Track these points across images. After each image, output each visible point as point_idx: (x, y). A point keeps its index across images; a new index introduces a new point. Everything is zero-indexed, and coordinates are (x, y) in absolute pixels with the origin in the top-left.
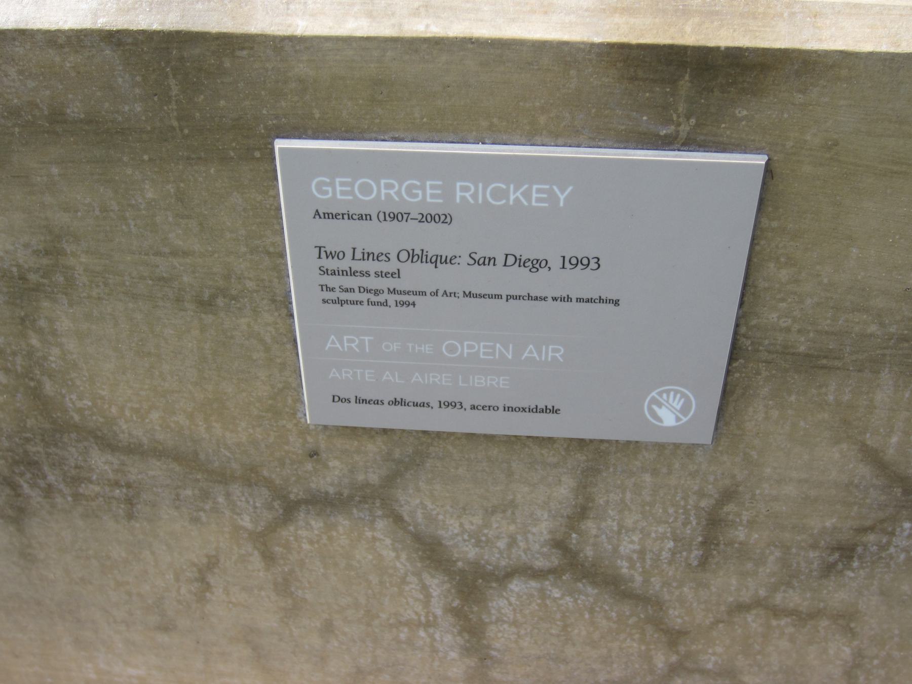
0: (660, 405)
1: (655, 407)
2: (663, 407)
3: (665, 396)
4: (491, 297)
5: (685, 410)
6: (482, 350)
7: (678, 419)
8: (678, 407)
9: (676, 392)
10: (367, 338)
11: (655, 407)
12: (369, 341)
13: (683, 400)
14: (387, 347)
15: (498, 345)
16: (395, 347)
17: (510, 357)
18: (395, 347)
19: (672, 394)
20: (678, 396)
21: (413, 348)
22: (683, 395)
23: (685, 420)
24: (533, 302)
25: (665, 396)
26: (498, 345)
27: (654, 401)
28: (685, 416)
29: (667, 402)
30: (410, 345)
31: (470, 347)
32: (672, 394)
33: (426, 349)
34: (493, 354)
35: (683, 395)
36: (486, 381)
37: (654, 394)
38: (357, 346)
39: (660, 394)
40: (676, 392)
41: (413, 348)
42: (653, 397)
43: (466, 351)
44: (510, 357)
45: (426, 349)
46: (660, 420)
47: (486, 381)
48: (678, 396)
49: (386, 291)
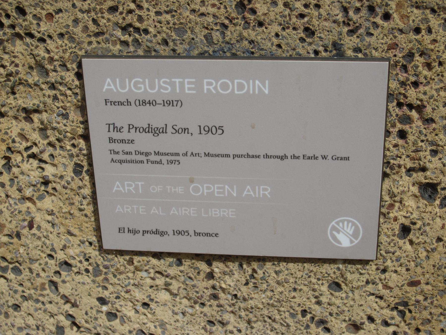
0: (338, 231)
1: (335, 233)
2: (341, 233)
3: (341, 224)
4: (223, 156)
5: (355, 234)
6: (216, 190)
7: (352, 242)
8: (351, 233)
9: (349, 221)
10: (140, 183)
11: (335, 233)
12: (141, 185)
13: (353, 228)
14: (154, 189)
15: (226, 187)
16: (158, 189)
17: (235, 195)
18: (158, 189)
19: (346, 223)
20: (350, 224)
21: (171, 189)
22: (354, 224)
23: (356, 242)
24: (251, 159)
25: (341, 224)
26: (226, 187)
27: (334, 228)
28: (356, 239)
29: (343, 229)
30: (169, 187)
31: (208, 188)
32: (346, 223)
33: (180, 190)
34: (223, 193)
35: (354, 224)
36: (220, 212)
37: (333, 223)
38: (133, 189)
39: (338, 223)
40: (349, 221)
41: (171, 189)
42: (333, 226)
43: (205, 191)
44: (235, 195)
45: (180, 190)
46: (339, 242)
47: (220, 212)
48: (350, 224)
49: (153, 153)
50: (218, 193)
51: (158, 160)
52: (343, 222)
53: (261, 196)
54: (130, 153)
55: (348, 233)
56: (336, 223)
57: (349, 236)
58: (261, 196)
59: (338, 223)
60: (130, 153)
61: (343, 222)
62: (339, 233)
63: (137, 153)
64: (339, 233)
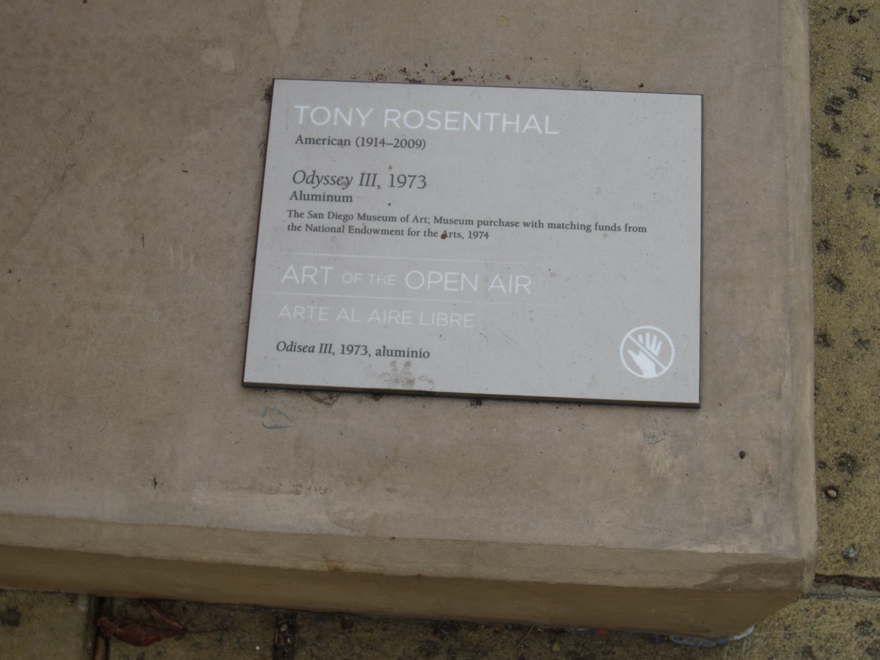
0: (637, 350)
1: (631, 352)
3: (640, 337)
6: (447, 281)
8: (656, 352)
11: (631, 352)
13: (660, 343)
15: (463, 275)
17: (475, 289)
19: (648, 335)
20: (655, 338)
22: (660, 337)
25: (640, 337)
26: (463, 275)
27: (630, 345)
29: (644, 345)
32: (648, 335)
37: (629, 335)
39: (635, 335)
40: (653, 333)
46: (638, 370)
49: (356, 216)
50: (450, 285)
51: (361, 227)
52: (643, 333)
53: (517, 291)
54: (321, 216)
55: (653, 355)
56: (633, 335)
57: (654, 358)
58: (517, 291)
59: (635, 335)
60: (321, 216)
61: (643, 333)
62: (637, 353)
63: (331, 215)
64: (637, 353)
